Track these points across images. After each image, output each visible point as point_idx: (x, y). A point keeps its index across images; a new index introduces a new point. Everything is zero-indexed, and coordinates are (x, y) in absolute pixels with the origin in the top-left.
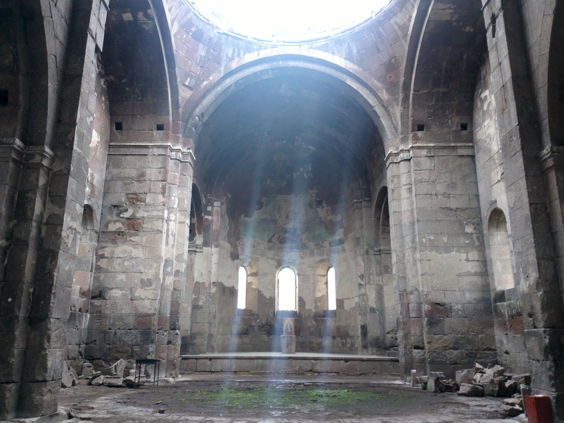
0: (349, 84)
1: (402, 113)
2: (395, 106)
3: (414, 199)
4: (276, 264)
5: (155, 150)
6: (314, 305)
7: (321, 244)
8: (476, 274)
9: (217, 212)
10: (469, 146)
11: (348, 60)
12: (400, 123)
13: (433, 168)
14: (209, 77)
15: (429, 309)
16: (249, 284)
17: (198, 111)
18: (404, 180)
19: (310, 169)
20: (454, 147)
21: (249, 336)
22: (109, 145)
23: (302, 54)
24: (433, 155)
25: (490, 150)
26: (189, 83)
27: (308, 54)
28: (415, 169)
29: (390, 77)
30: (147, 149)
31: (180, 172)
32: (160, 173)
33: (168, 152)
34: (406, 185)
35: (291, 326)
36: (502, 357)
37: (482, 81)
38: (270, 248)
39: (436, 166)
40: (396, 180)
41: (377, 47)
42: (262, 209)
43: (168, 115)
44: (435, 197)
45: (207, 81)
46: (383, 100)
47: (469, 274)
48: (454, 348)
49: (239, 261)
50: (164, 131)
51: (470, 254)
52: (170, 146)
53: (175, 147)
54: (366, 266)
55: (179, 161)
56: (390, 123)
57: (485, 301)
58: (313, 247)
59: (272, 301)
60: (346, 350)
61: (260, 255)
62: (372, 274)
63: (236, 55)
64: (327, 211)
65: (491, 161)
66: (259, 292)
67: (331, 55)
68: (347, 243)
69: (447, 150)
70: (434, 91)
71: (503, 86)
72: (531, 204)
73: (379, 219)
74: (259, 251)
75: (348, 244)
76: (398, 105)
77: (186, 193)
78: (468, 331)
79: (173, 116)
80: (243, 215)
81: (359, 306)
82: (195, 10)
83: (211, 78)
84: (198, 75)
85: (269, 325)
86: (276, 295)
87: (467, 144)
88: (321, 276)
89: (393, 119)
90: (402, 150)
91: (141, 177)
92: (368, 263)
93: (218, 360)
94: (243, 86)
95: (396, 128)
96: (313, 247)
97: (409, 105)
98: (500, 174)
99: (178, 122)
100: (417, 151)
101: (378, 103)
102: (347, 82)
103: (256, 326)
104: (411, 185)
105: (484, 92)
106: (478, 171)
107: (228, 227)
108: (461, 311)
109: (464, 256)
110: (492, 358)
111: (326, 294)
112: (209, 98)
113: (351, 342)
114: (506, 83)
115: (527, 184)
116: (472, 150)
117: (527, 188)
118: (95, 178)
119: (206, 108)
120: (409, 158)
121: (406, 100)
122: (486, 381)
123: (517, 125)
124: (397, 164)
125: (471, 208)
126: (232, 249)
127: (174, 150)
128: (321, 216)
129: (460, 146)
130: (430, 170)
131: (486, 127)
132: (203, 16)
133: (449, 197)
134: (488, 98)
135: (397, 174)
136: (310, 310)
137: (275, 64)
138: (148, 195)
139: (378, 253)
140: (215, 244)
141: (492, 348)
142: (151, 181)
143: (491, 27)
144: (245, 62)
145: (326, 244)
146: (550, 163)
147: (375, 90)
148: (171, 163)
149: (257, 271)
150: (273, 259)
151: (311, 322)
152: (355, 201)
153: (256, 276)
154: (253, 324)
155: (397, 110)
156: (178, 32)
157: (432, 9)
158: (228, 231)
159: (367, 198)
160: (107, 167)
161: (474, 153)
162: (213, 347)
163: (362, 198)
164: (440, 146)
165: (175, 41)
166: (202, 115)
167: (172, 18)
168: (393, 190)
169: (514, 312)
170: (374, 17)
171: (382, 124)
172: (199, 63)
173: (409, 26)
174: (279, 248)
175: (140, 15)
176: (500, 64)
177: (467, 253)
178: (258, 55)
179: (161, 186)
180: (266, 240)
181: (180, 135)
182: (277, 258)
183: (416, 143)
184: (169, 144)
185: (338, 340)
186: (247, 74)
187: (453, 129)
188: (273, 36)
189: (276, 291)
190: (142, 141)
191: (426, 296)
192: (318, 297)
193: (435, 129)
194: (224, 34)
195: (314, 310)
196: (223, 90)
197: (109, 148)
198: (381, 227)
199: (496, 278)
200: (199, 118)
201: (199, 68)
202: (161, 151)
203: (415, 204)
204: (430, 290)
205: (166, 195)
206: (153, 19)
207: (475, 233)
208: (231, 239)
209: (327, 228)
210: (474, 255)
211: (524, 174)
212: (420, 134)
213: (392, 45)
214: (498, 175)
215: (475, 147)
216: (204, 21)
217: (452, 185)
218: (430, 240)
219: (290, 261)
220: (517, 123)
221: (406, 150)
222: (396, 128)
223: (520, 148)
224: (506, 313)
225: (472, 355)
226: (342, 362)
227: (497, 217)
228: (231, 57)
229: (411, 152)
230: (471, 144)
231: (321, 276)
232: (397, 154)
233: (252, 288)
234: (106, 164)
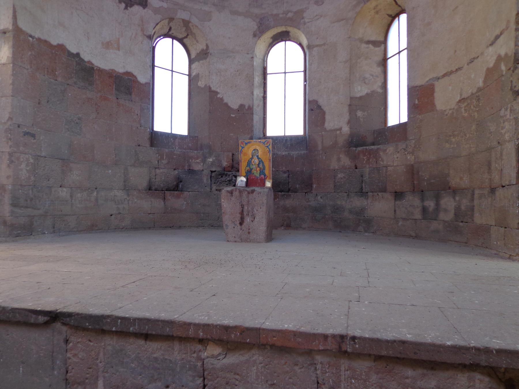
4: (253, 25)
6: (346, 117)
21: (186, 193)
35: (261, 161)
61: (214, 5)
66: (213, 94)
86: (257, 103)
88: (368, 42)
103: (206, 172)
111: (380, 91)
113: (458, 209)
149: (207, 46)
153: (205, 58)
154: (197, 167)
182: (257, 11)
189: (257, 92)
192: (358, 95)
195: (346, 129)
219: (290, 15)
231: (368, 42)
233: (199, 87)
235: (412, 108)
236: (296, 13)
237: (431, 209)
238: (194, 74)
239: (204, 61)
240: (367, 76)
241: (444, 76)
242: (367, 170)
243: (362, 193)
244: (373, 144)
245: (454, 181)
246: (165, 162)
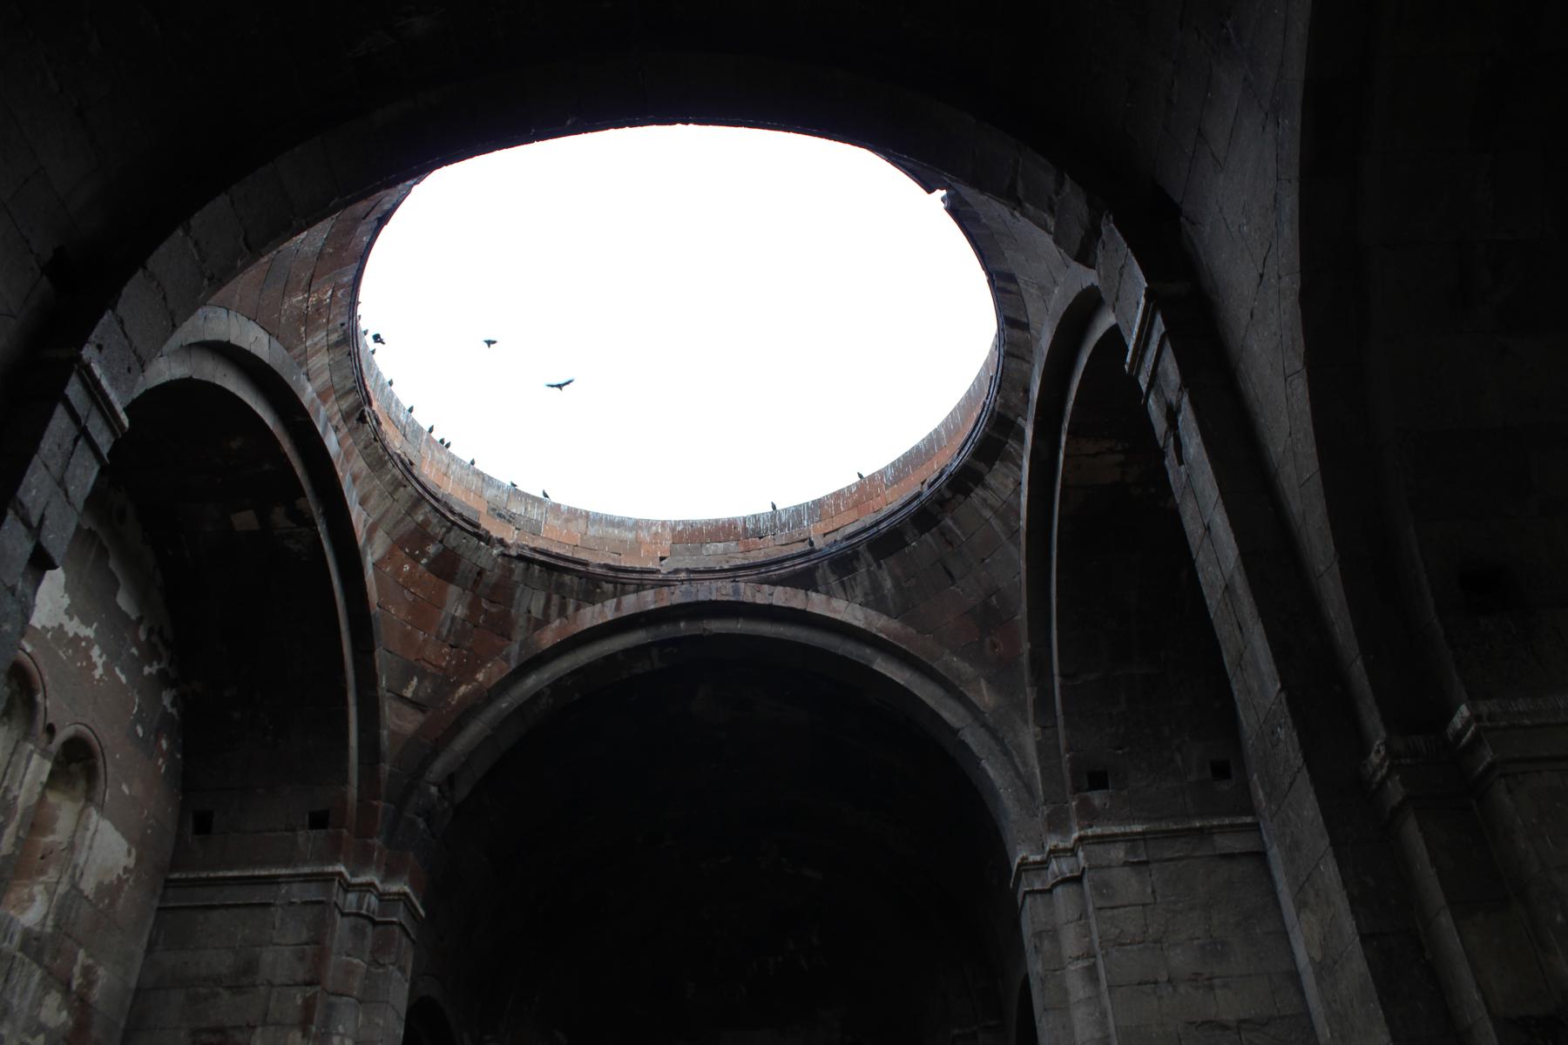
0: (882, 671)
1: (1038, 744)
3: (1106, 1001)
5: (296, 887)
11: (871, 608)
12: (1038, 771)
13: (1150, 900)
14: (475, 673)
17: (439, 767)
20: (1201, 829)
22: (168, 881)
23: (741, 599)
24: (1144, 858)
26: (414, 693)
27: (760, 599)
28: (1098, 905)
29: (994, 646)
30: (274, 888)
31: (367, 957)
32: (301, 959)
33: (335, 891)
34: (1078, 958)
40: (1047, 944)
41: (945, 568)
43: (345, 781)
44: (1170, 989)
45: (468, 685)
46: (982, 709)
50: (330, 830)
52: (340, 874)
53: (357, 876)
55: (366, 922)
63: (554, 610)
67: (824, 597)
71: (1227, 587)
72: (1365, 939)
76: (1026, 722)
77: (381, 1022)
79: (359, 787)
82: (437, 500)
83: (480, 677)
84: (441, 667)
89: (1017, 760)
90: (1051, 852)
91: (244, 976)
94: (577, 696)
95: (1029, 788)
97: (1056, 717)
99: (375, 803)
100: (1097, 848)
101: (969, 720)
102: (875, 667)
104: (1094, 956)
112: (475, 730)
114: (1232, 577)
115: (1340, 870)
117: (1345, 885)
118: (100, 983)
119: (463, 759)
120: (1076, 874)
121: (1044, 704)
123: (1280, 690)
124: (1047, 897)
127: (354, 885)
129: (1219, 826)
130: (1144, 905)
132: (460, 515)
133: (1211, 988)
135: (1049, 927)
137: (666, 631)
138: (259, 1030)
142: (271, 984)
143: (1172, 439)
144: (580, 629)
146: (1396, 792)
147: (957, 683)
148: (342, 925)
152: (956, 1031)
155: (1028, 737)
156: (389, 556)
157: (1066, 456)
160: (150, 949)
161: (1263, 842)
164: (1163, 832)
165: (378, 579)
166: (450, 780)
167: (371, 520)
168: (1043, 981)
170: (926, 492)
171: (988, 777)
172: (448, 636)
173: (1019, 504)
175: (279, 516)
176: (1208, 529)
178: (618, 607)
179: (299, 1002)
181: (377, 842)
183: (1091, 826)
184: (342, 869)
186: (587, 661)
188: (662, 559)
190: (262, 864)
194: (520, 558)
196: (516, 705)
197: (165, 888)
200: (439, 790)
201: (446, 650)
202: (313, 892)
203: (1110, 1018)
205: (314, 1029)
206: (312, 524)
211: (1327, 841)
212: (1097, 798)
213: (983, 560)
215: (1262, 825)
216: (462, 529)
220: (1279, 686)
221: (1065, 850)
223: (1300, 762)
228: (540, 617)
229: (1081, 854)
230: (1249, 820)
232: (1043, 865)
234: (145, 940)
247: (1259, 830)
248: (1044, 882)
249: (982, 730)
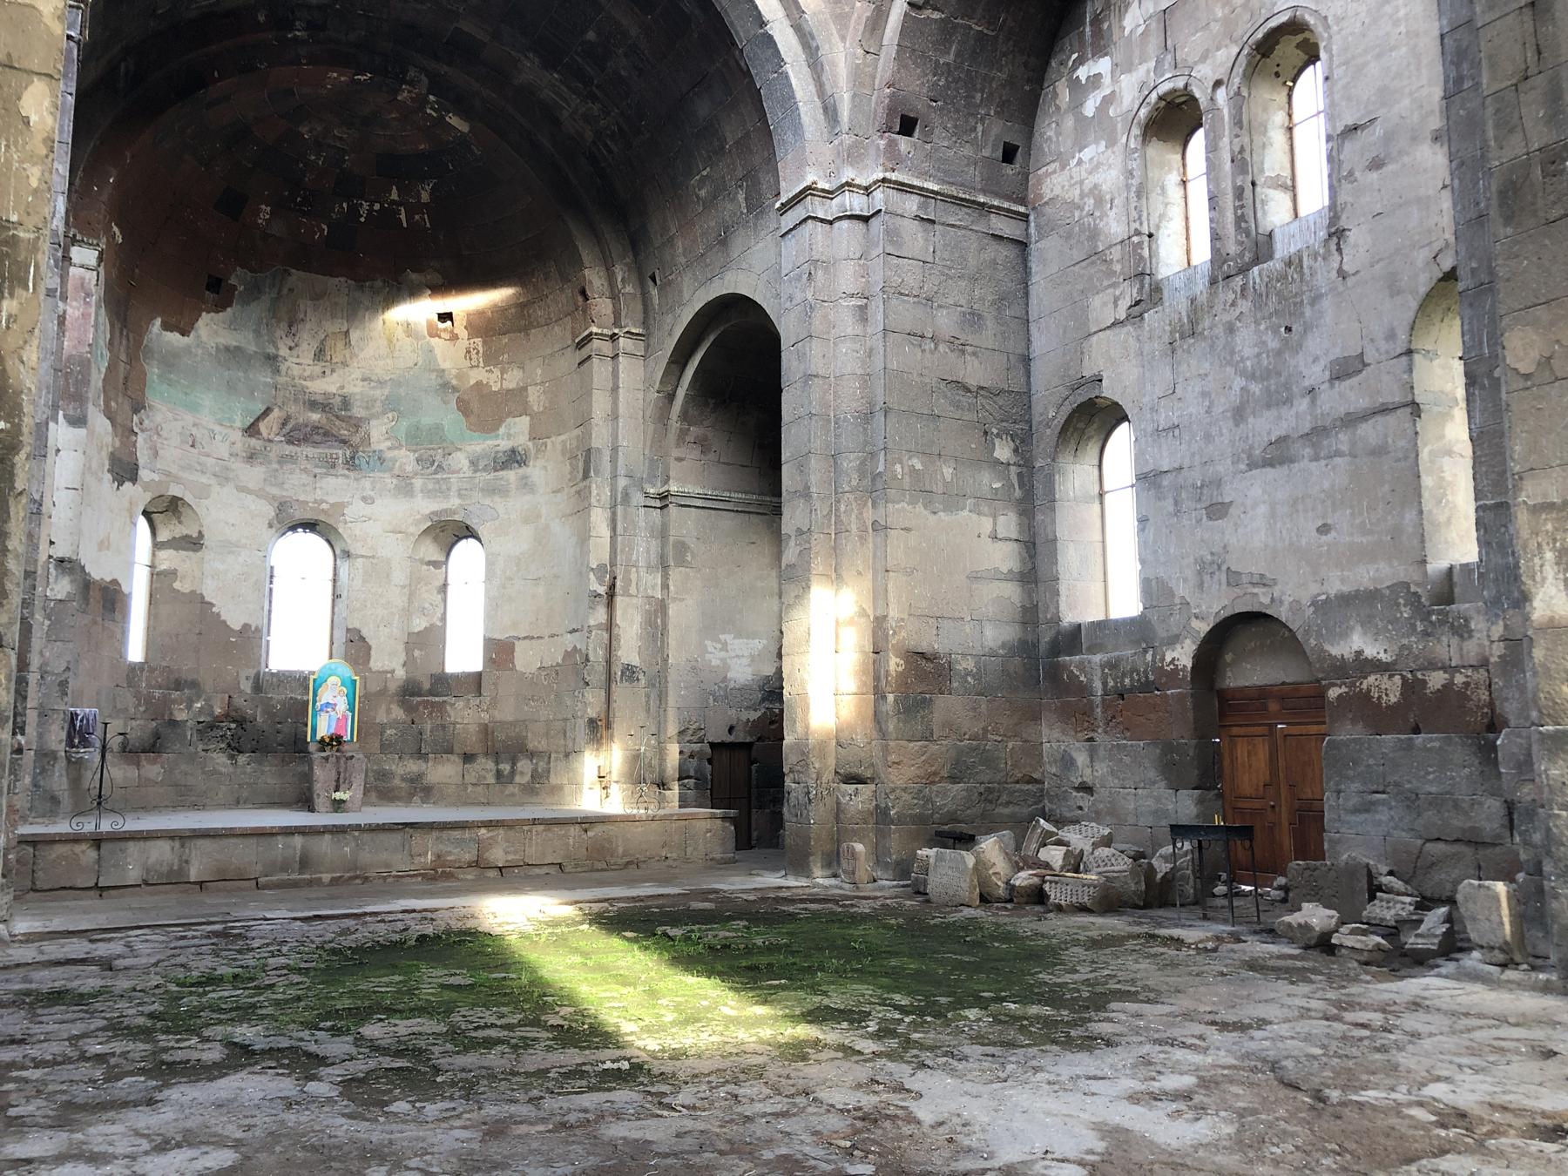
2: (836, 38)
6: (402, 657)
7: (438, 458)
8: (1009, 577)
9: (82, 284)
10: (1018, 213)
12: (847, 96)
15: (900, 669)
16: (160, 580)
18: (847, 279)
19: (425, 197)
20: (983, 205)
25: (1094, 234)
34: (852, 296)
36: (1065, 799)
37: (1088, 29)
38: (251, 457)
39: (938, 253)
42: (229, 309)
44: (932, 345)
47: (997, 576)
48: (953, 779)
49: (138, 487)
51: (1001, 519)
54: (619, 538)
56: (812, 88)
57: (1025, 649)
58: (409, 468)
59: (251, 639)
60: (513, 795)
62: (637, 567)
64: (468, 352)
65: (1093, 263)
68: (540, 463)
69: (966, 210)
70: (959, 21)
73: (671, 397)
74: (210, 461)
75: (545, 468)
76: (843, 38)
78: (985, 730)
80: (158, 322)
81: (587, 660)
85: (234, 721)
87: (1015, 207)
88: (429, 563)
90: (848, 184)
92: (625, 529)
93: (131, 844)
95: (830, 111)
96: (409, 468)
98: (1125, 303)
105: (1091, 62)
106: (1033, 290)
107: (107, 354)
108: (973, 677)
109: (986, 524)
110: (1035, 803)
113: (535, 771)
116: (1022, 225)
122: (1116, 868)
125: (1010, 392)
126: (118, 444)
128: (446, 365)
129: (998, 208)
131: (1086, 166)
134: (1107, 80)
135: (824, 259)
136: (387, 672)
139: (658, 503)
140: (71, 412)
141: (1035, 776)
145: (460, 460)
149: (200, 532)
150: (260, 494)
151: (389, 711)
152: (595, 329)
153: (196, 551)
154: (181, 716)
155: (841, 55)
158: (108, 368)
159: (635, 327)
161: (1028, 235)
162: (54, 800)
163: (617, 324)
169: (1127, 681)
174: (283, 460)
177: (995, 517)
180: (238, 424)
182: (275, 491)
185: (485, 766)
187: (986, 153)
191: (895, 633)
193: (941, 139)
195: (401, 673)
198: (675, 423)
199: (1063, 589)
204: (906, 617)
207: (1014, 464)
208: (113, 404)
209: (464, 407)
210: (1009, 523)
212: (904, 143)
214: (1116, 306)
215: (1032, 218)
217: (973, 319)
218: (913, 469)
219: (324, 506)
221: (859, 187)
222: (830, 111)
224: (1098, 685)
225: (990, 797)
226: (574, 831)
227: (1081, 425)
229: (878, 195)
230: (1022, 209)
231: (429, 563)
232: (828, 194)
235: (489, 661)
236: (333, 505)
237: (506, 773)
238: (163, 567)
239: (191, 554)
240: (427, 605)
241: (525, 638)
242: (428, 727)
243: (420, 755)
244: (431, 693)
245: (532, 744)
246: (142, 709)
247: (1027, 222)
248: (826, 211)
249: (791, 30)
